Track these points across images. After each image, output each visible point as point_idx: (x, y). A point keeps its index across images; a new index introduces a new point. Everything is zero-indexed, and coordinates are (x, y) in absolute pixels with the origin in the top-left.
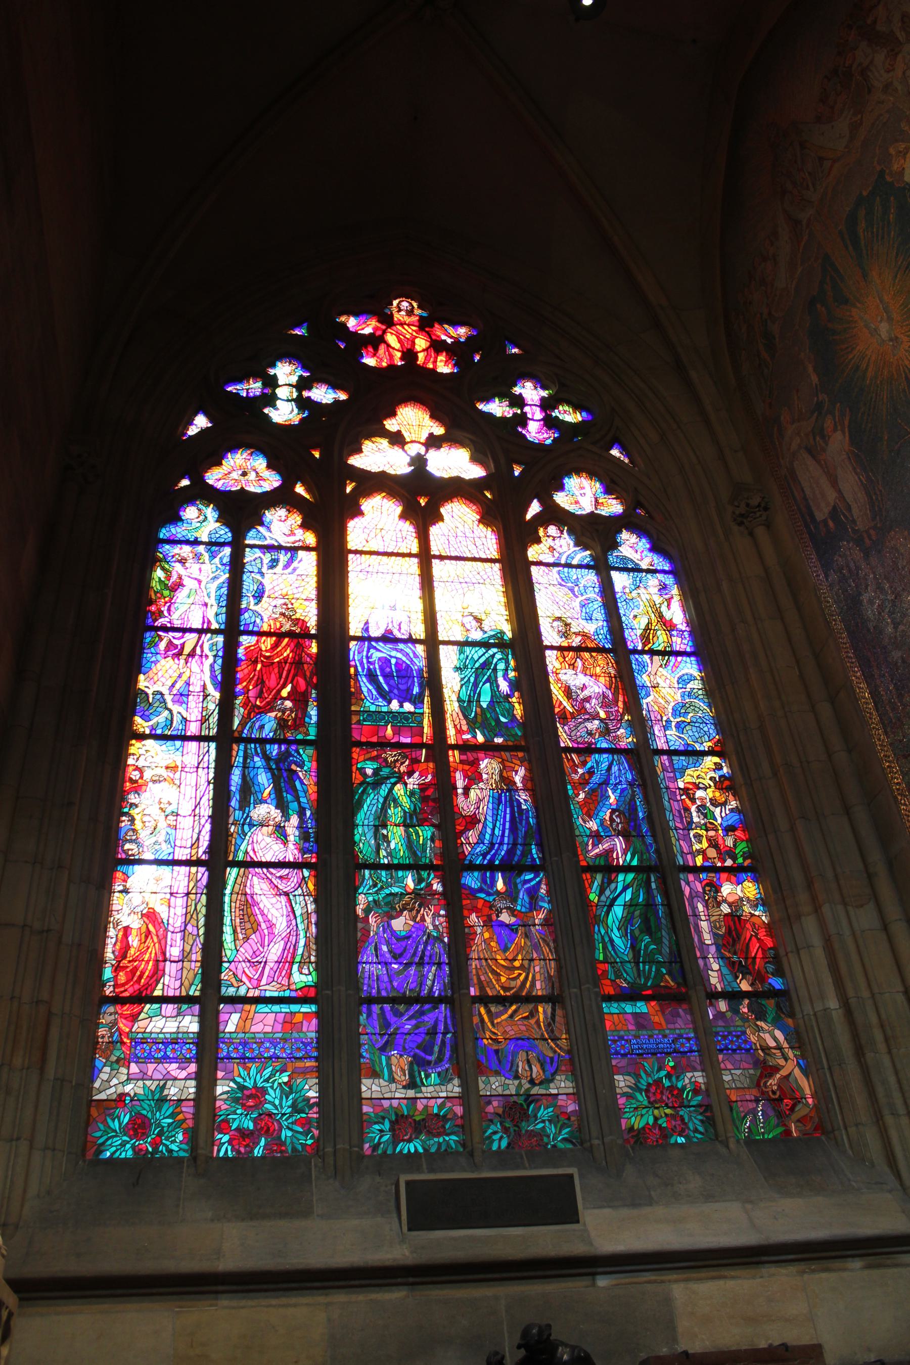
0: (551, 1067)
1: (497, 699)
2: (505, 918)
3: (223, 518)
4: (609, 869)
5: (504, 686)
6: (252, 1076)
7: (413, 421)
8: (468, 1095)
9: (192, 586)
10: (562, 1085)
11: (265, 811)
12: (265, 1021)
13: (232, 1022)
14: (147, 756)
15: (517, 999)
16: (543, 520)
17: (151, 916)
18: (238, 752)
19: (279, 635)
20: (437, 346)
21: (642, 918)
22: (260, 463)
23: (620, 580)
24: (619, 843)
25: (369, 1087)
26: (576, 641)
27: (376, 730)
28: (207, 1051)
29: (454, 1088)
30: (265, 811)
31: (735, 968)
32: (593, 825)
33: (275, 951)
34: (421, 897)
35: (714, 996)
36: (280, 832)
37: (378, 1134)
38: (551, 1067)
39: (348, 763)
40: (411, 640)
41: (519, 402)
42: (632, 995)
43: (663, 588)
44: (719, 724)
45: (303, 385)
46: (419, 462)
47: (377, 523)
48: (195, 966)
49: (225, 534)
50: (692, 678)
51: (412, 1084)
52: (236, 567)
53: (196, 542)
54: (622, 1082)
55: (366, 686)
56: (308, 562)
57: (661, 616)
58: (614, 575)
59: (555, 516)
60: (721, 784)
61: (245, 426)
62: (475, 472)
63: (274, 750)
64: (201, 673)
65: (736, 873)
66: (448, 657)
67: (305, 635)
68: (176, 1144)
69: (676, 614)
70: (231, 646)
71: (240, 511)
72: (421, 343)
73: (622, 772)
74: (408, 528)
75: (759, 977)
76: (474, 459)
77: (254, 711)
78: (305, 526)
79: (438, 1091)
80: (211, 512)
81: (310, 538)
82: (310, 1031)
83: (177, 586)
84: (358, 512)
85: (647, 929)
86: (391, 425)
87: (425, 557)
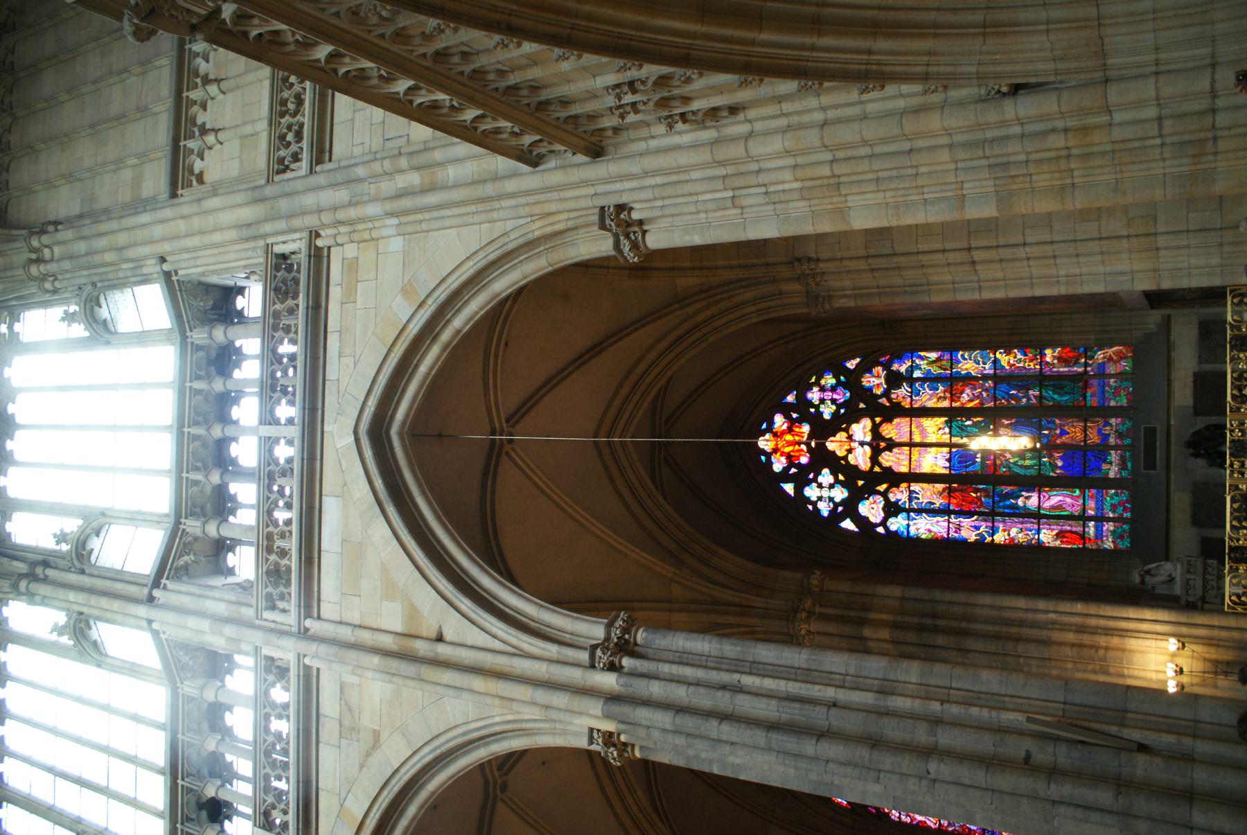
0: (1107, 424)
1: (975, 425)
2: (1058, 432)
3: (896, 516)
4: (1040, 397)
5: (968, 423)
6: (1107, 507)
7: (835, 444)
8: (1116, 448)
9: (924, 527)
10: (1113, 421)
11: (1020, 502)
12: (1091, 504)
13: (1091, 512)
14: (1000, 538)
15: (1085, 431)
16: (889, 400)
17: (1057, 535)
18: (997, 510)
19: (950, 496)
20: (790, 430)
21: (1059, 389)
22: (867, 502)
23: (917, 374)
24: (1031, 392)
25: (1112, 475)
26: (948, 395)
27: (988, 466)
28: (1100, 519)
29: (1113, 452)
30: (1020, 502)
31: (1076, 363)
32: (1024, 400)
33: (1068, 500)
34: (1050, 456)
35: (1086, 371)
36: (1028, 498)
37: (1124, 474)
38: (1107, 424)
39: (1002, 476)
40: (950, 452)
41: (822, 401)
42: (1085, 397)
43: (922, 358)
44: (983, 349)
45: (820, 486)
46: (862, 444)
47: (894, 460)
48: (1073, 523)
49: (904, 515)
50: (962, 356)
51: (1111, 463)
52: (919, 511)
53: (908, 526)
54: (1112, 403)
55: (971, 469)
56: (915, 487)
57: (933, 362)
58: (915, 375)
59: (886, 394)
60: (1008, 353)
61: (850, 508)
62: (866, 423)
63: (997, 499)
64: (966, 522)
65: (1043, 355)
66: (954, 440)
67: (949, 488)
68: (1126, 527)
69: (933, 356)
70: (954, 512)
71: (892, 509)
72: (789, 437)
73: (1003, 387)
74: (895, 450)
75: (1080, 356)
76: (857, 421)
77: (982, 505)
78: (898, 487)
79: (1114, 456)
80: (891, 520)
81: (904, 485)
82: (1094, 491)
83: (930, 531)
84: (890, 468)
85: (1062, 388)
86: (841, 453)
87: (911, 445)
